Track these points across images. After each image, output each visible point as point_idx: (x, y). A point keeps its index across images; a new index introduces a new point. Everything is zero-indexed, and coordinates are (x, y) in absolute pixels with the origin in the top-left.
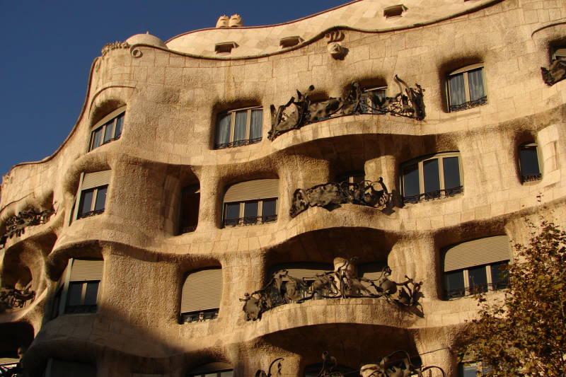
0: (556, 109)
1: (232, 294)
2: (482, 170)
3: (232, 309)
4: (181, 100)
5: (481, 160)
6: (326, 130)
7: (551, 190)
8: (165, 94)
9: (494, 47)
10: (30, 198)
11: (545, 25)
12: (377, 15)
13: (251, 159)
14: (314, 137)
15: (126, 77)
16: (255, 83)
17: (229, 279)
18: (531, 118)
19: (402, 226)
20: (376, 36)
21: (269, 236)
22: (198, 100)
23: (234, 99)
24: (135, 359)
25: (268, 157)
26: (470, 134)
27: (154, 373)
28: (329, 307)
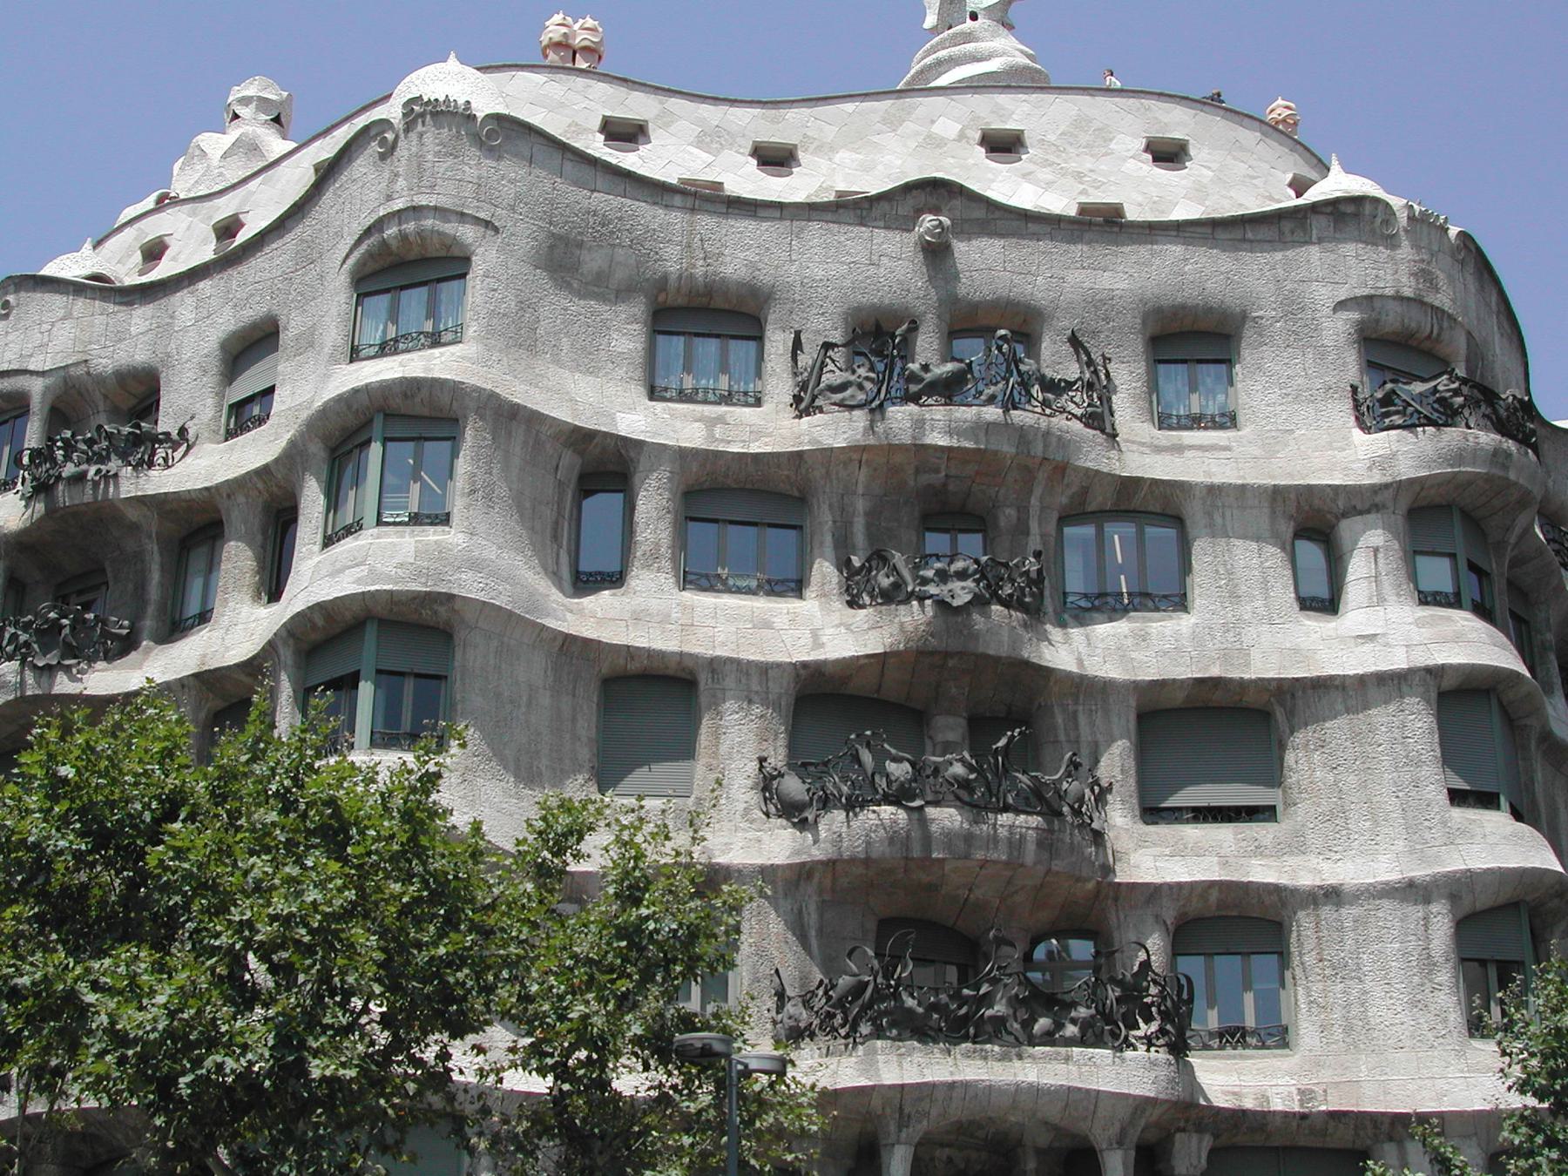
0: (1386, 486)
1: (723, 749)
4: (585, 269)
6: (939, 426)
7: (1368, 647)
9: (1261, 313)
10: (81, 370)
11: (1360, 292)
12: (962, 136)
13: (755, 448)
15: (468, 191)
16: (752, 265)
18: (1336, 489)
19: (1080, 662)
21: (807, 639)
22: (620, 275)
25: (800, 454)
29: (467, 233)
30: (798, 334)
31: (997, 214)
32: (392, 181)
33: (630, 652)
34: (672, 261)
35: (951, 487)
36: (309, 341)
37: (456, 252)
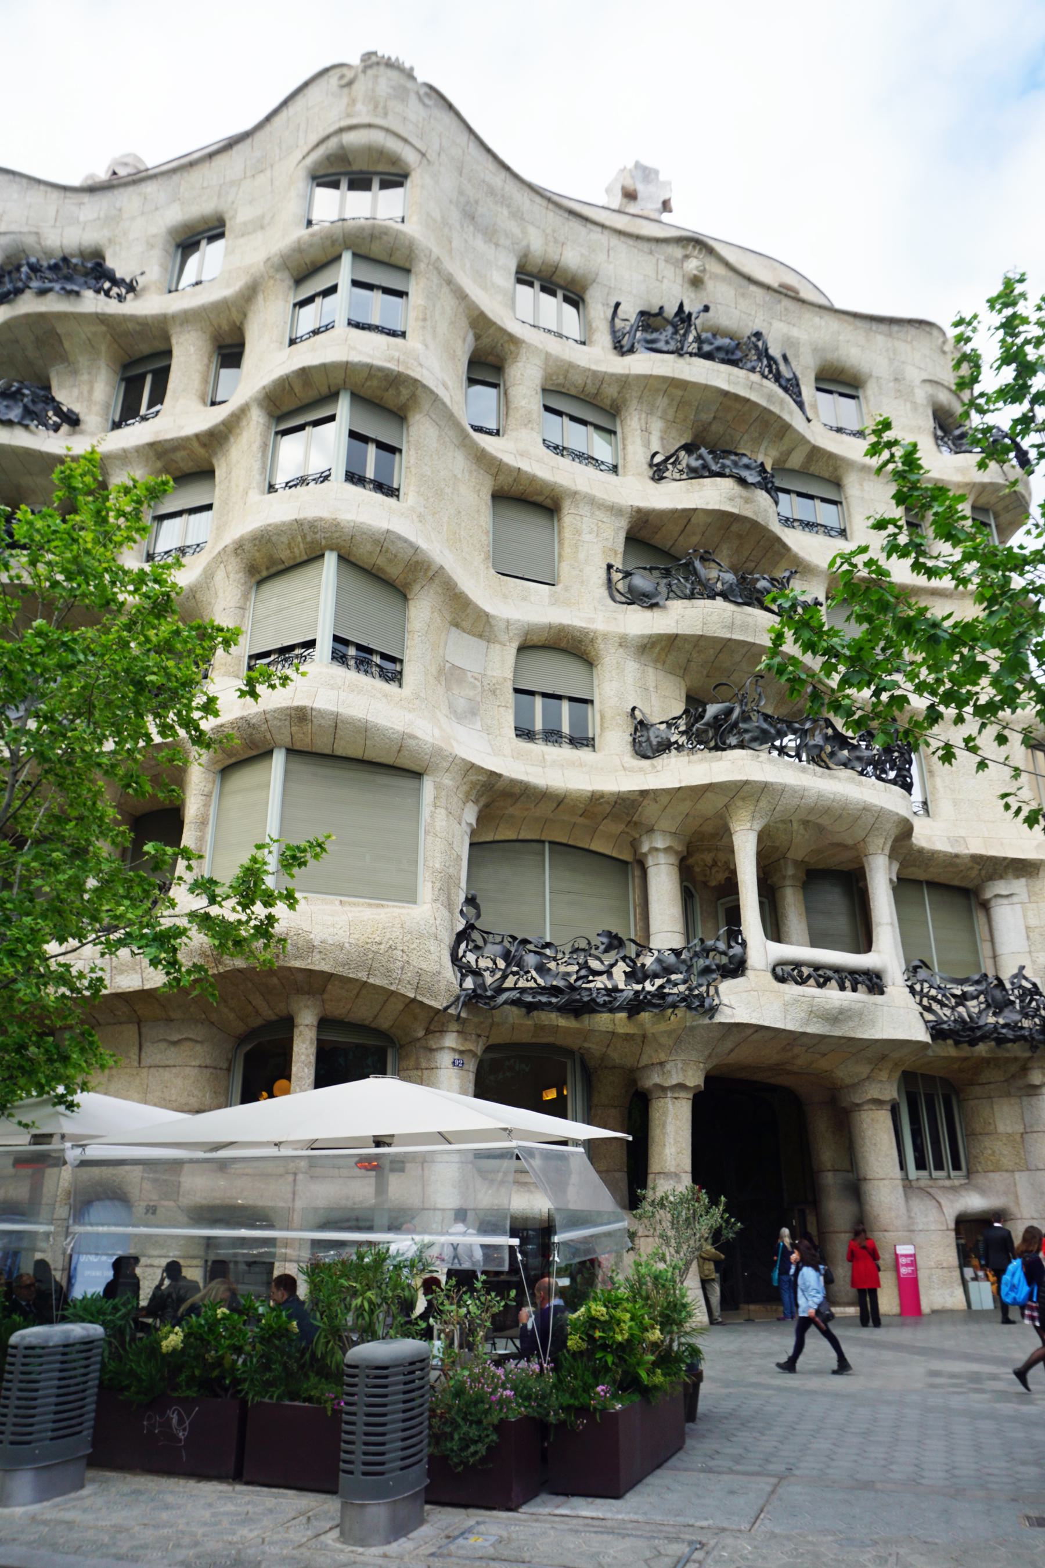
0: (967, 484)
1: (582, 556)
17: (578, 532)
20: (745, 283)
30: (618, 305)
32: (353, 102)
35: (714, 427)
36: (260, 225)
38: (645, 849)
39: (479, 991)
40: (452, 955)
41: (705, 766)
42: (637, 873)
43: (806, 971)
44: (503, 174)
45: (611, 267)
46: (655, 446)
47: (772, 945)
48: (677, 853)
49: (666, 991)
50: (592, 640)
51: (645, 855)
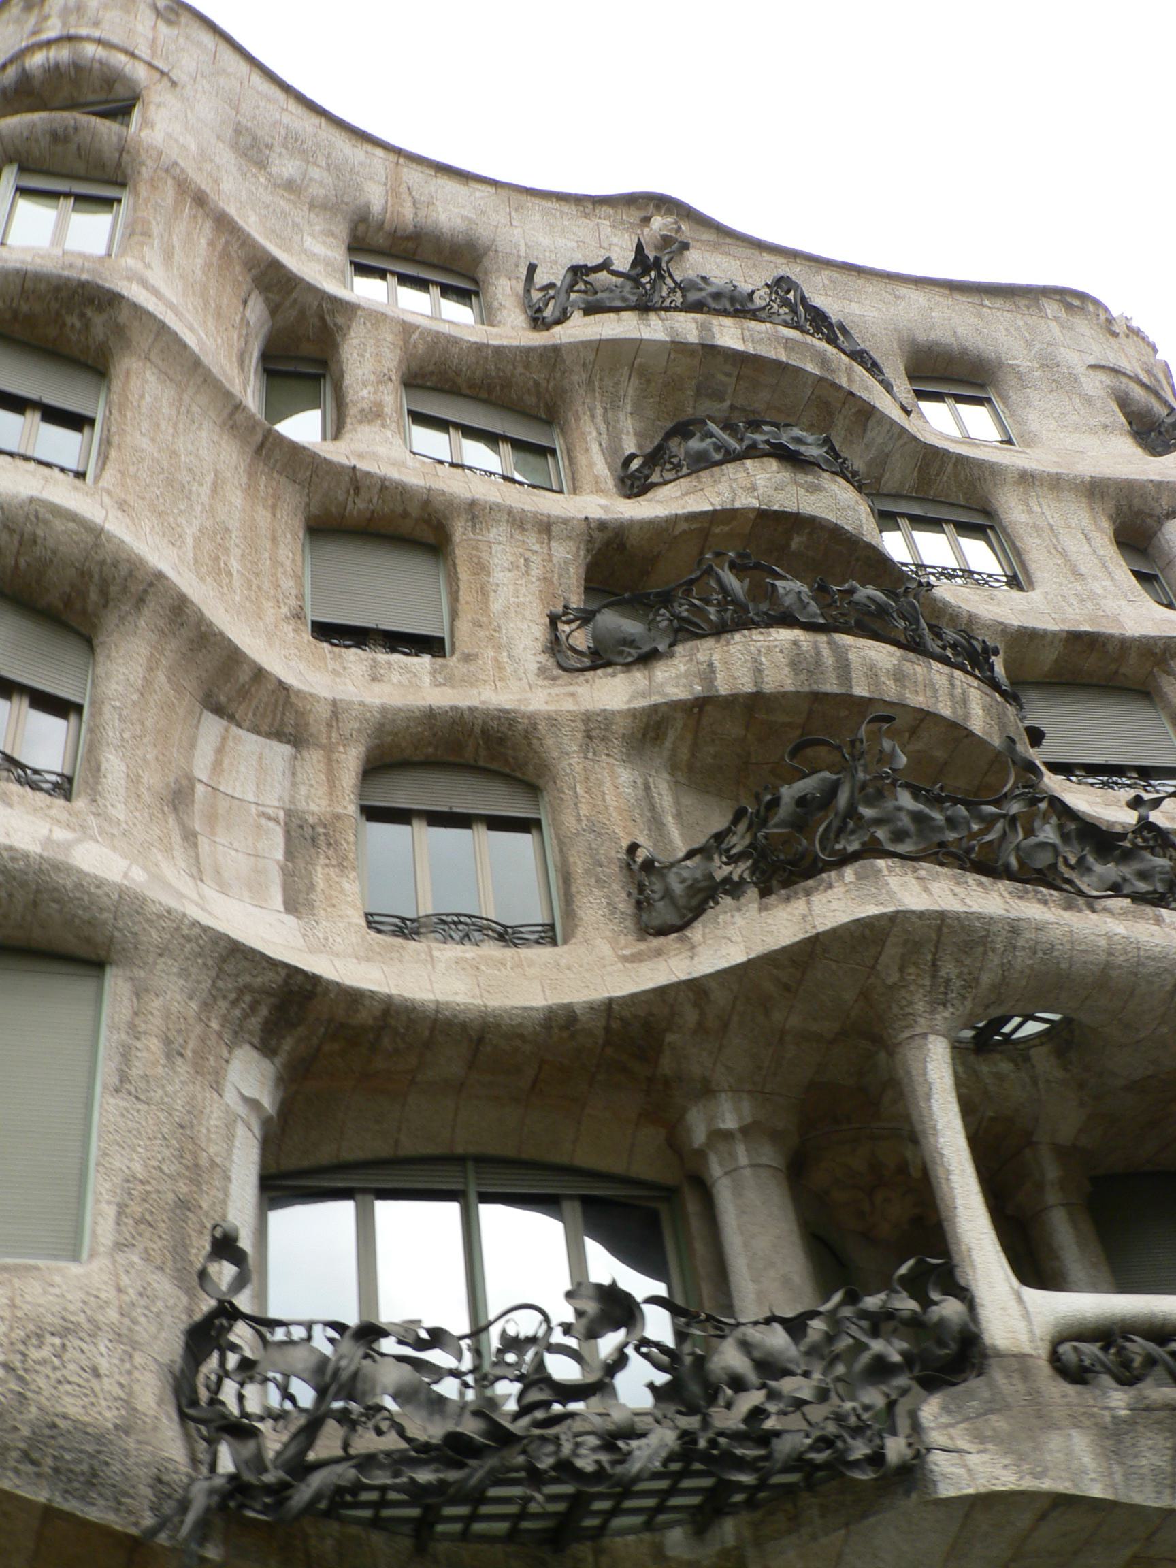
1: (496, 606)
2: (1063, 554)
3: (527, 635)
4: (274, 170)
5: (1058, 540)
8: (238, 132)
9: (1016, 362)
11: (1103, 363)
14: (701, 337)
17: (481, 568)
18: (1159, 485)
22: (314, 190)
23: (411, 228)
24: (233, 657)
26: (1026, 479)
27: (268, 735)
28: (908, 664)
29: (140, 73)
30: (532, 269)
31: (728, 240)
33: (355, 480)
34: (375, 197)
37: (120, 91)
38: (699, 1136)
39: (249, 1477)
40: (178, 1391)
41: (799, 906)
42: (692, 1206)
43: (1138, 1347)
44: (315, 120)
45: (516, 231)
46: (630, 446)
47: (1035, 1297)
48: (775, 1136)
49: (769, 1424)
50: (527, 735)
51: (701, 1154)
